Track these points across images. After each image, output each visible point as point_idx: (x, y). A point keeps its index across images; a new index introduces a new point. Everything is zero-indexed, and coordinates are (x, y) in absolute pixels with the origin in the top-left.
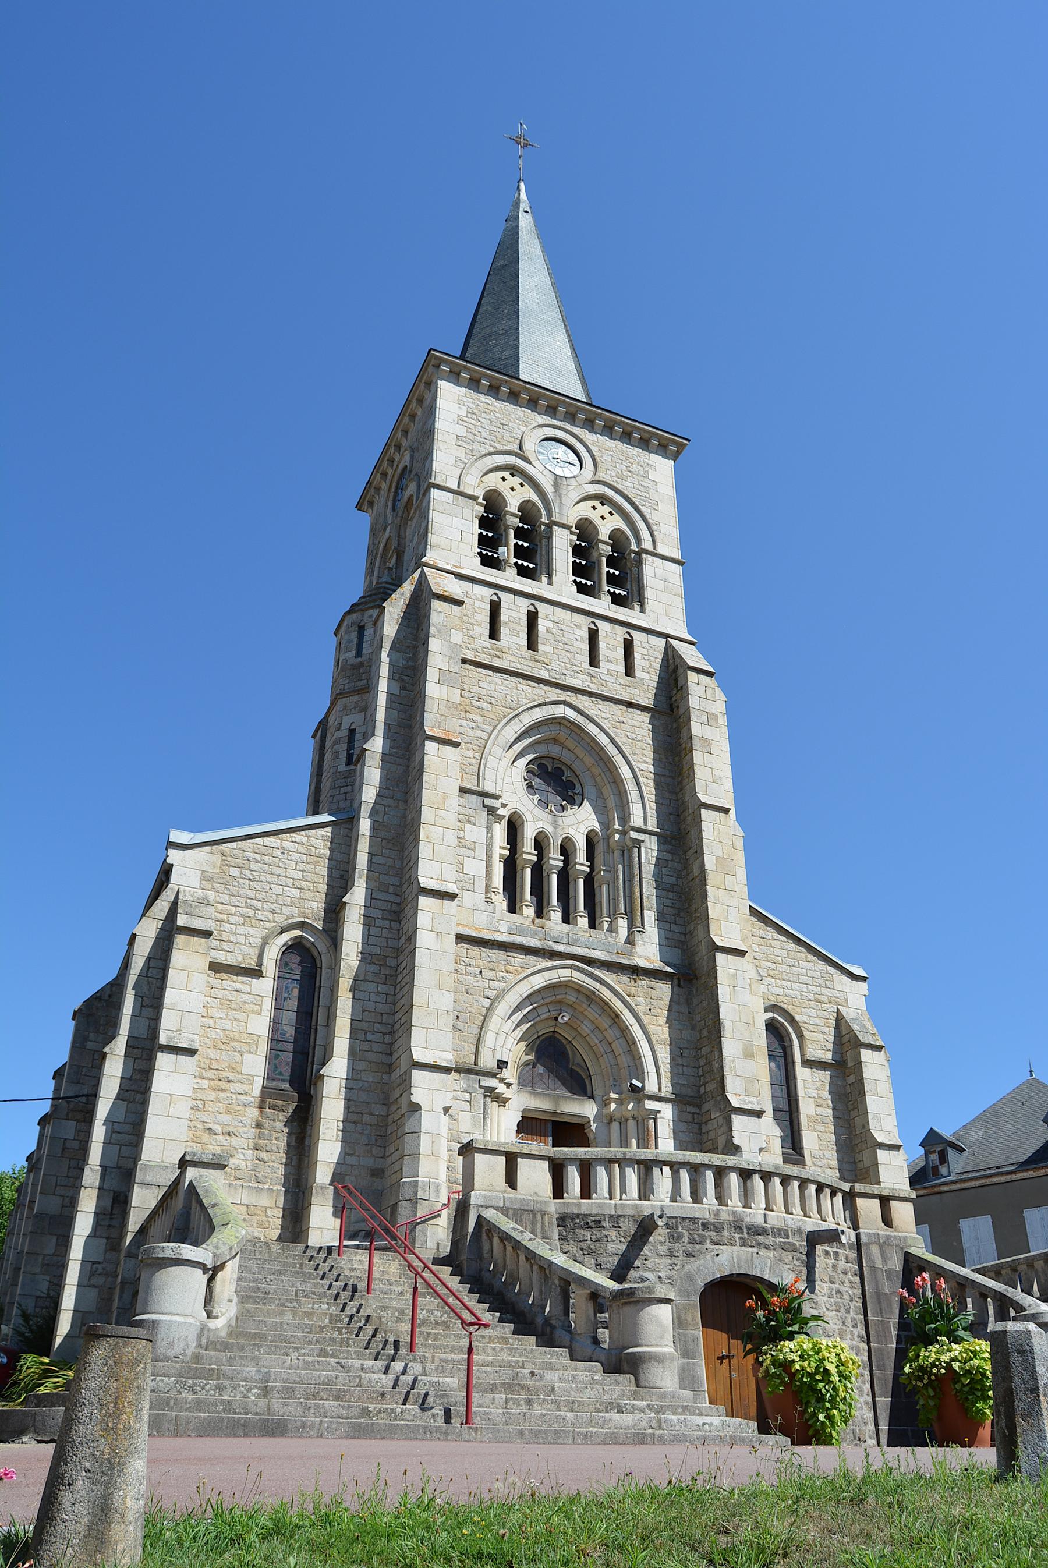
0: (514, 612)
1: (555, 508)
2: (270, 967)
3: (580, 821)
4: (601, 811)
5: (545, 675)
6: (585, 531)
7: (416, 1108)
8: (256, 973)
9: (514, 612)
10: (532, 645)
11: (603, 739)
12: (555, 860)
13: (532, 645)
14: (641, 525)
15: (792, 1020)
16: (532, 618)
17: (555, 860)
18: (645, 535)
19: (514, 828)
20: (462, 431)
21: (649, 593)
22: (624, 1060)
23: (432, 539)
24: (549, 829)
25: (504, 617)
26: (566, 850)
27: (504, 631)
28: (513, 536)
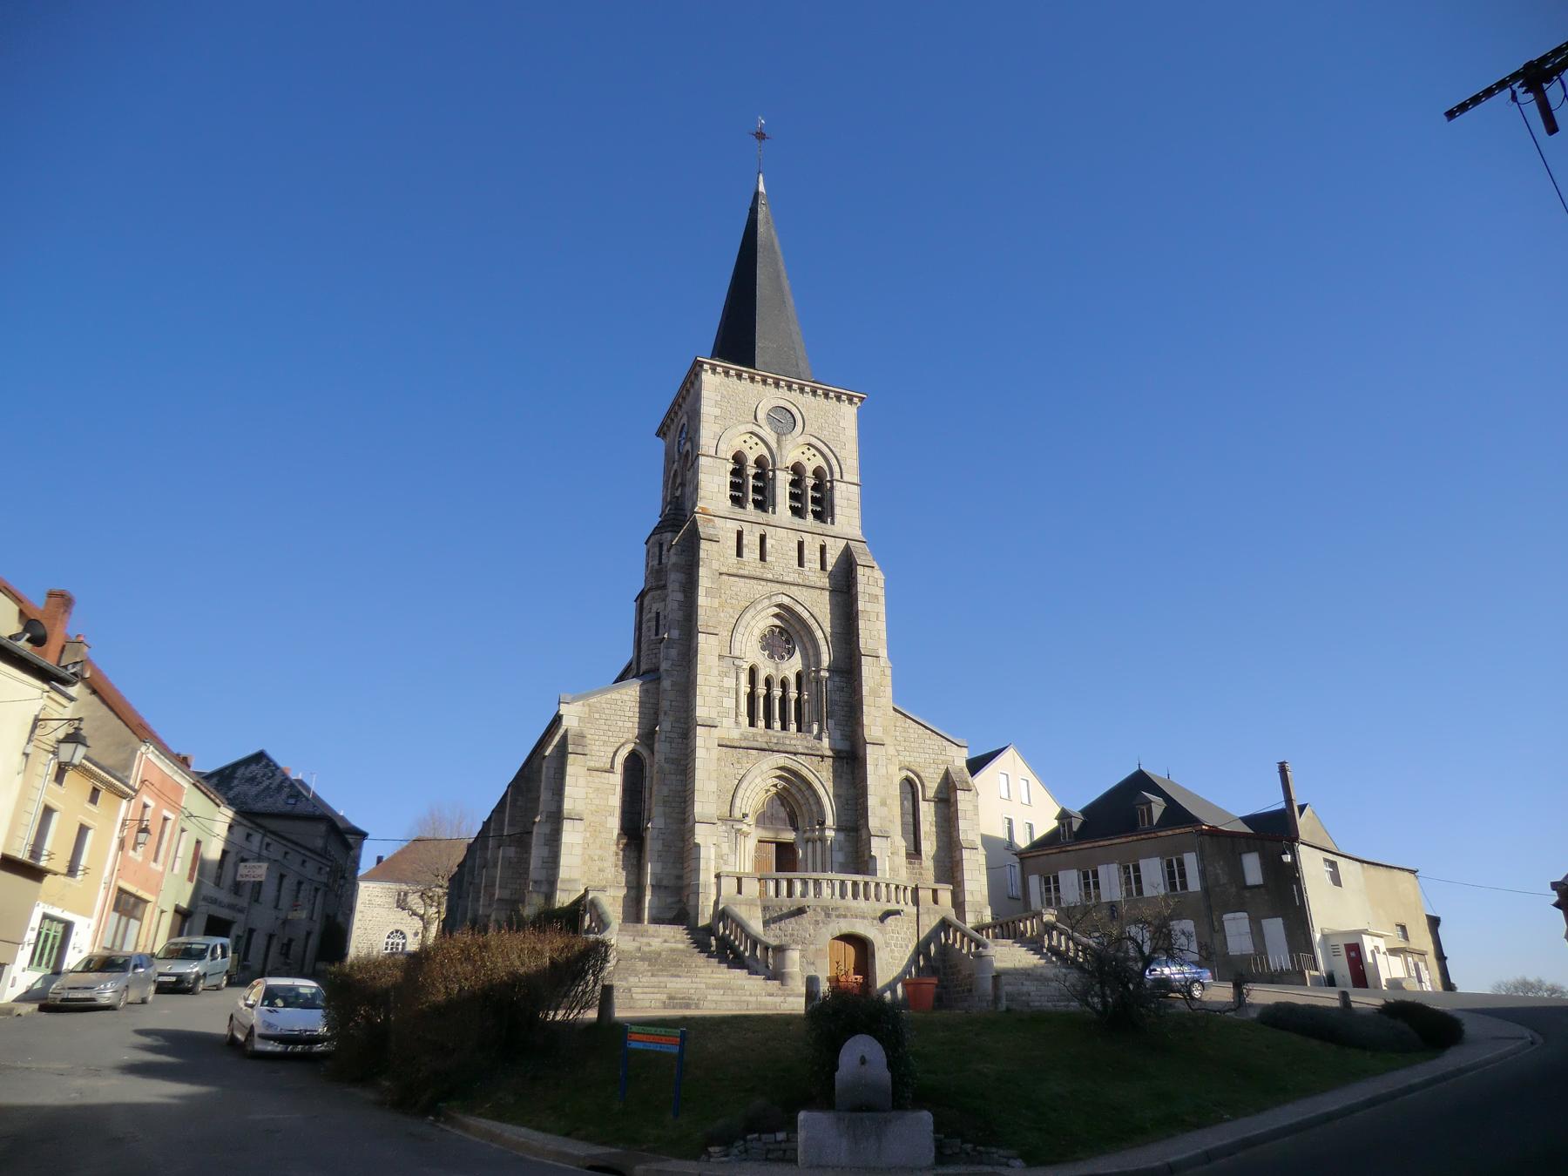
0: (751, 540)
1: (778, 459)
2: (619, 767)
3: (792, 666)
4: (805, 656)
5: (770, 576)
6: (797, 469)
7: (698, 846)
8: (611, 770)
9: (751, 540)
10: (763, 558)
11: (805, 615)
12: (777, 692)
13: (763, 558)
14: (834, 462)
15: (918, 776)
16: (763, 539)
17: (777, 692)
18: (836, 469)
19: (753, 672)
20: (717, 412)
21: (837, 510)
22: (814, 808)
23: (701, 493)
24: (774, 673)
25: (745, 542)
26: (784, 684)
27: (745, 550)
28: (751, 484)
